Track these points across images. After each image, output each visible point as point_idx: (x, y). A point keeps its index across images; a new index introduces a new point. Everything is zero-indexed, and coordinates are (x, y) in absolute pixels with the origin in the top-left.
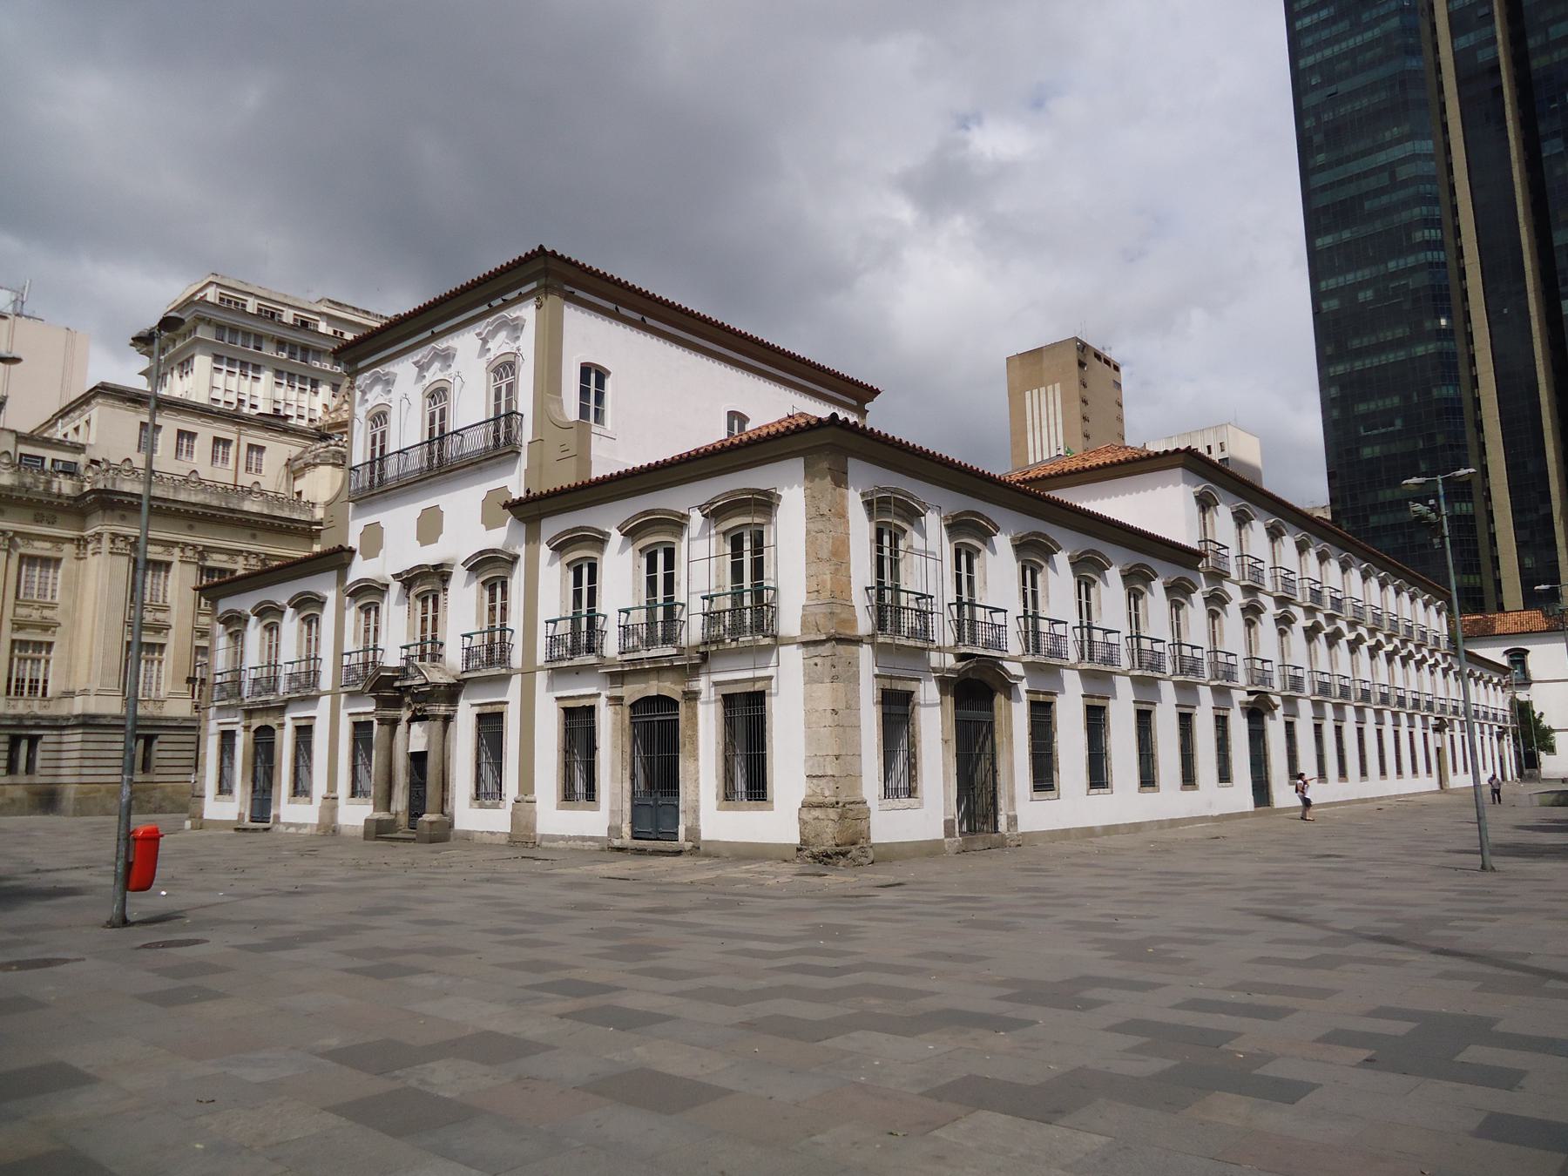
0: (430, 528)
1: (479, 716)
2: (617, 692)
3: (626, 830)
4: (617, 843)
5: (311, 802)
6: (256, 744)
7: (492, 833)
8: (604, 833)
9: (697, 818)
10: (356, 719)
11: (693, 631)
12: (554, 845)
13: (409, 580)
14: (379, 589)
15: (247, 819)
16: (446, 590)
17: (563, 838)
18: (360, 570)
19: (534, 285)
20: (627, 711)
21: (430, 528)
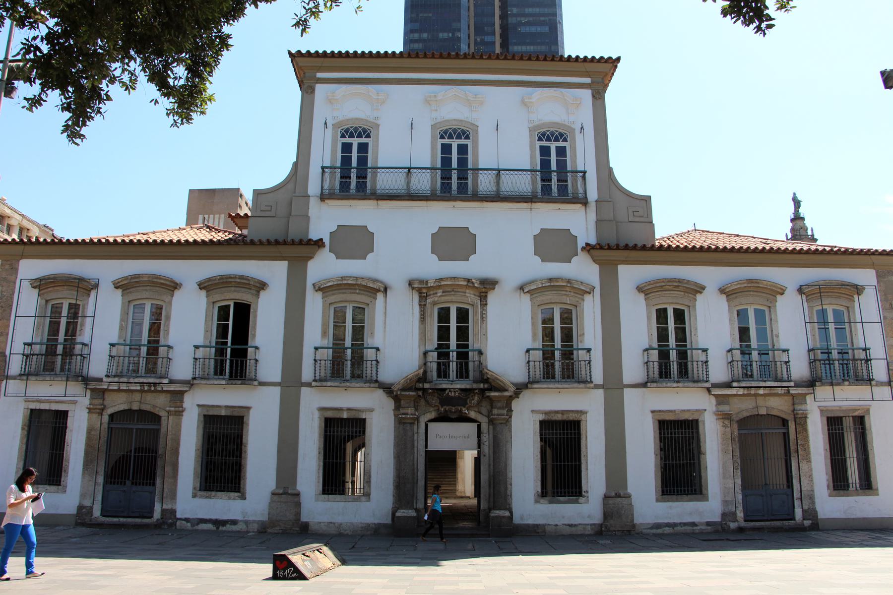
0: (454, 243)
1: (542, 423)
2: (725, 408)
3: (740, 514)
4: (733, 525)
5: (243, 498)
6: (110, 430)
7: (571, 525)
8: (717, 519)
9: (813, 503)
10: (330, 414)
11: (799, 368)
12: (660, 531)
13: (422, 289)
14: (375, 289)
15: (97, 512)
16: (484, 304)
17: (668, 525)
18: (324, 266)
19: (588, 80)
20: (735, 426)
21: (454, 243)
